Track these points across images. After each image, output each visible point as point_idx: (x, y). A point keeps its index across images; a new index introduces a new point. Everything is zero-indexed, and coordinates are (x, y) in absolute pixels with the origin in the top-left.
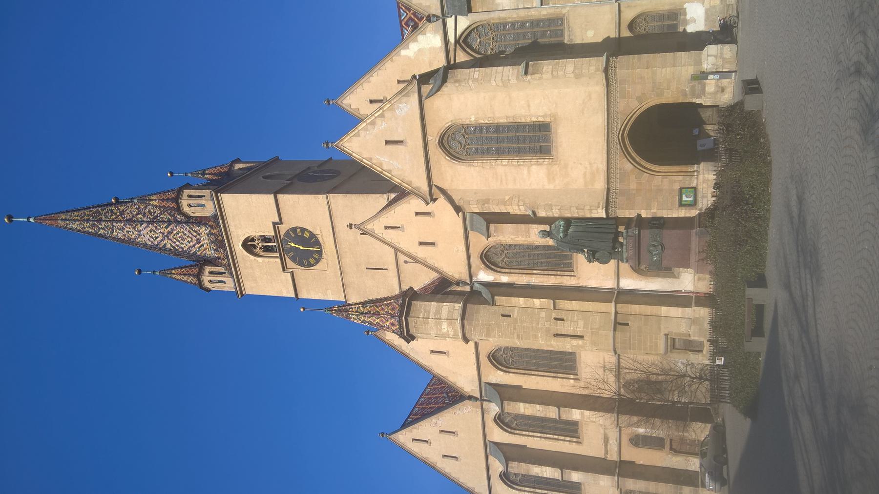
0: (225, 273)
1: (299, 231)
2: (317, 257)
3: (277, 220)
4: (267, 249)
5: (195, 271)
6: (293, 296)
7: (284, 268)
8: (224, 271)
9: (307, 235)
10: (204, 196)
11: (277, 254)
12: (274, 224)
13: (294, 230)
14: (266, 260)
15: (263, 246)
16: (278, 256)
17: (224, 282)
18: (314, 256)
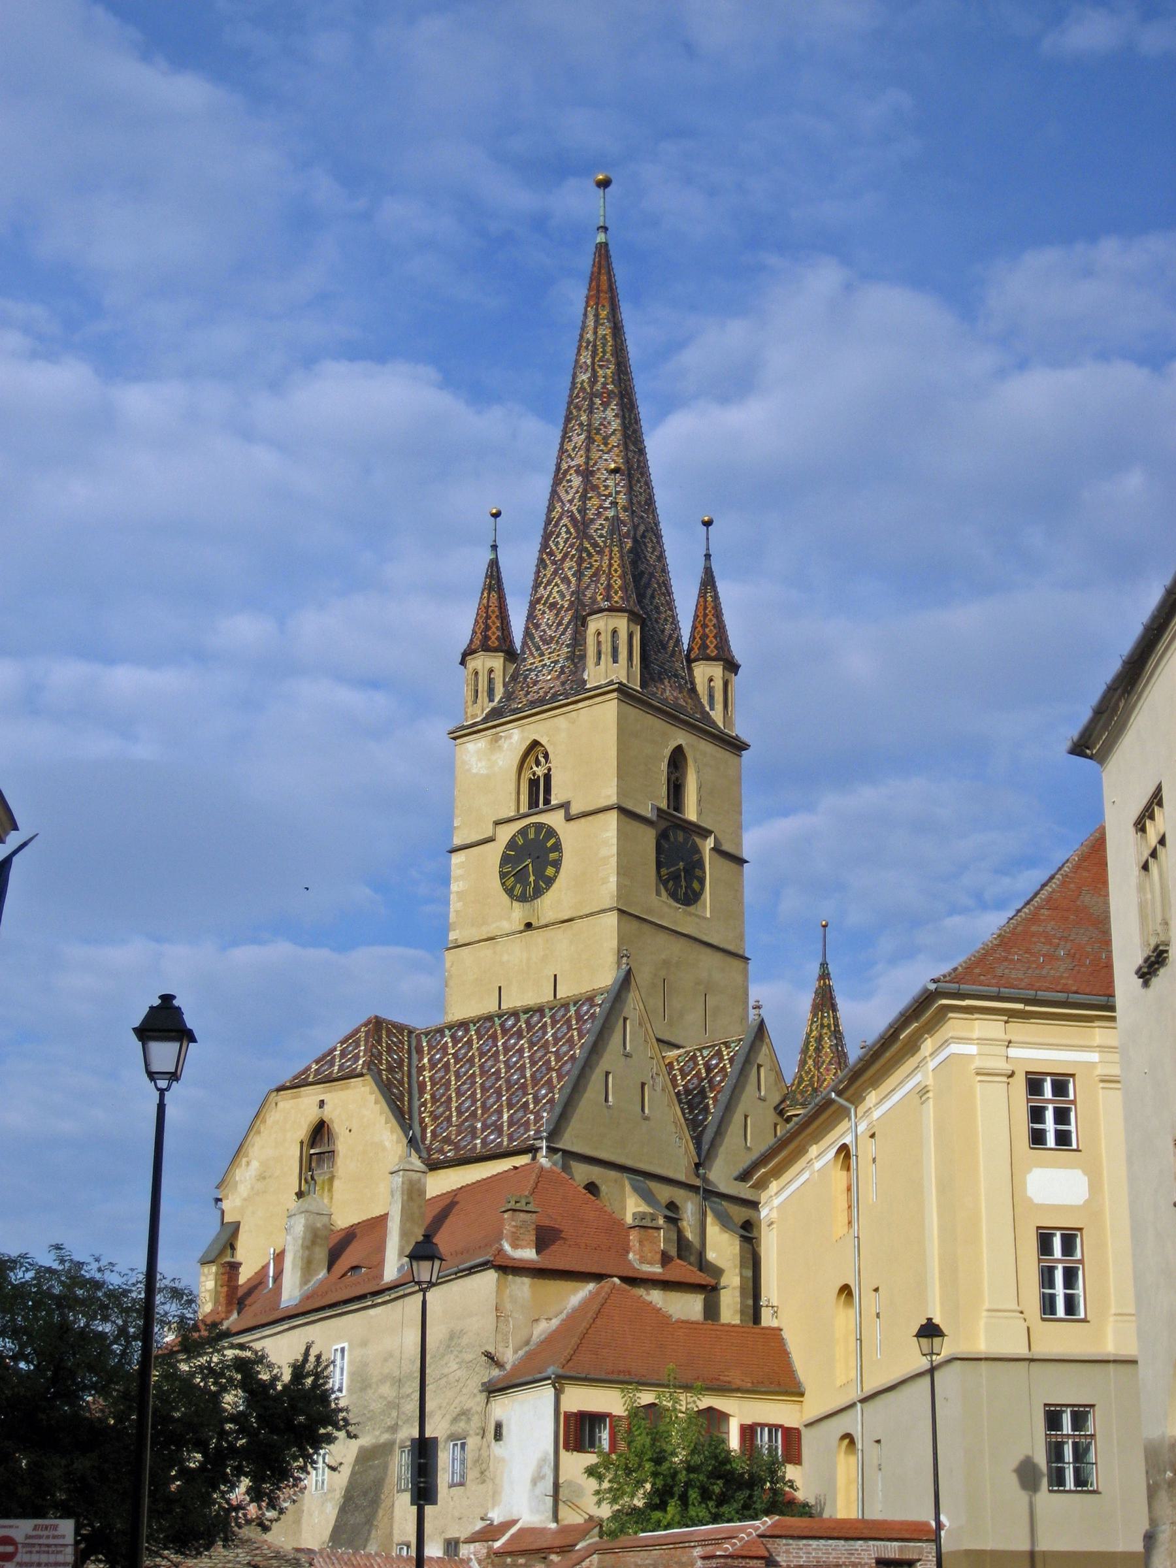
0: (491, 700)
1: (553, 856)
2: (515, 893)
3: (574, 810)
4: (534, 783)
5: (494, 634)
6: (457, 841)
7: (497, 823)
8: (498, 696)
9: (550, 871)
10: (615, 661)
11: (524, 809)
12: (565, 806)
13: (557, 847)
14: (512, 787)
15: (539, 777)
16: (522, 811)
17: (475, 702)
18: (518, 885)
